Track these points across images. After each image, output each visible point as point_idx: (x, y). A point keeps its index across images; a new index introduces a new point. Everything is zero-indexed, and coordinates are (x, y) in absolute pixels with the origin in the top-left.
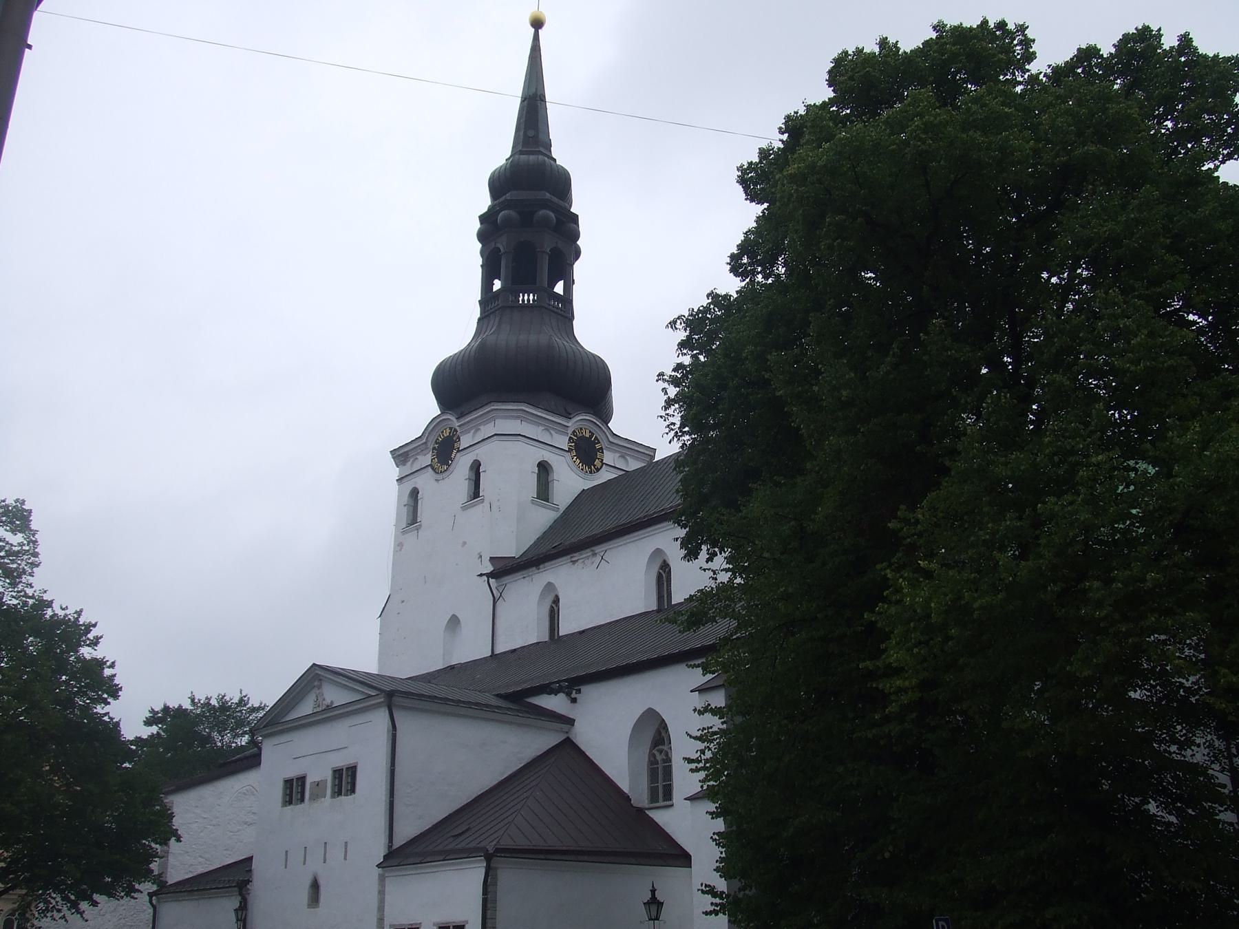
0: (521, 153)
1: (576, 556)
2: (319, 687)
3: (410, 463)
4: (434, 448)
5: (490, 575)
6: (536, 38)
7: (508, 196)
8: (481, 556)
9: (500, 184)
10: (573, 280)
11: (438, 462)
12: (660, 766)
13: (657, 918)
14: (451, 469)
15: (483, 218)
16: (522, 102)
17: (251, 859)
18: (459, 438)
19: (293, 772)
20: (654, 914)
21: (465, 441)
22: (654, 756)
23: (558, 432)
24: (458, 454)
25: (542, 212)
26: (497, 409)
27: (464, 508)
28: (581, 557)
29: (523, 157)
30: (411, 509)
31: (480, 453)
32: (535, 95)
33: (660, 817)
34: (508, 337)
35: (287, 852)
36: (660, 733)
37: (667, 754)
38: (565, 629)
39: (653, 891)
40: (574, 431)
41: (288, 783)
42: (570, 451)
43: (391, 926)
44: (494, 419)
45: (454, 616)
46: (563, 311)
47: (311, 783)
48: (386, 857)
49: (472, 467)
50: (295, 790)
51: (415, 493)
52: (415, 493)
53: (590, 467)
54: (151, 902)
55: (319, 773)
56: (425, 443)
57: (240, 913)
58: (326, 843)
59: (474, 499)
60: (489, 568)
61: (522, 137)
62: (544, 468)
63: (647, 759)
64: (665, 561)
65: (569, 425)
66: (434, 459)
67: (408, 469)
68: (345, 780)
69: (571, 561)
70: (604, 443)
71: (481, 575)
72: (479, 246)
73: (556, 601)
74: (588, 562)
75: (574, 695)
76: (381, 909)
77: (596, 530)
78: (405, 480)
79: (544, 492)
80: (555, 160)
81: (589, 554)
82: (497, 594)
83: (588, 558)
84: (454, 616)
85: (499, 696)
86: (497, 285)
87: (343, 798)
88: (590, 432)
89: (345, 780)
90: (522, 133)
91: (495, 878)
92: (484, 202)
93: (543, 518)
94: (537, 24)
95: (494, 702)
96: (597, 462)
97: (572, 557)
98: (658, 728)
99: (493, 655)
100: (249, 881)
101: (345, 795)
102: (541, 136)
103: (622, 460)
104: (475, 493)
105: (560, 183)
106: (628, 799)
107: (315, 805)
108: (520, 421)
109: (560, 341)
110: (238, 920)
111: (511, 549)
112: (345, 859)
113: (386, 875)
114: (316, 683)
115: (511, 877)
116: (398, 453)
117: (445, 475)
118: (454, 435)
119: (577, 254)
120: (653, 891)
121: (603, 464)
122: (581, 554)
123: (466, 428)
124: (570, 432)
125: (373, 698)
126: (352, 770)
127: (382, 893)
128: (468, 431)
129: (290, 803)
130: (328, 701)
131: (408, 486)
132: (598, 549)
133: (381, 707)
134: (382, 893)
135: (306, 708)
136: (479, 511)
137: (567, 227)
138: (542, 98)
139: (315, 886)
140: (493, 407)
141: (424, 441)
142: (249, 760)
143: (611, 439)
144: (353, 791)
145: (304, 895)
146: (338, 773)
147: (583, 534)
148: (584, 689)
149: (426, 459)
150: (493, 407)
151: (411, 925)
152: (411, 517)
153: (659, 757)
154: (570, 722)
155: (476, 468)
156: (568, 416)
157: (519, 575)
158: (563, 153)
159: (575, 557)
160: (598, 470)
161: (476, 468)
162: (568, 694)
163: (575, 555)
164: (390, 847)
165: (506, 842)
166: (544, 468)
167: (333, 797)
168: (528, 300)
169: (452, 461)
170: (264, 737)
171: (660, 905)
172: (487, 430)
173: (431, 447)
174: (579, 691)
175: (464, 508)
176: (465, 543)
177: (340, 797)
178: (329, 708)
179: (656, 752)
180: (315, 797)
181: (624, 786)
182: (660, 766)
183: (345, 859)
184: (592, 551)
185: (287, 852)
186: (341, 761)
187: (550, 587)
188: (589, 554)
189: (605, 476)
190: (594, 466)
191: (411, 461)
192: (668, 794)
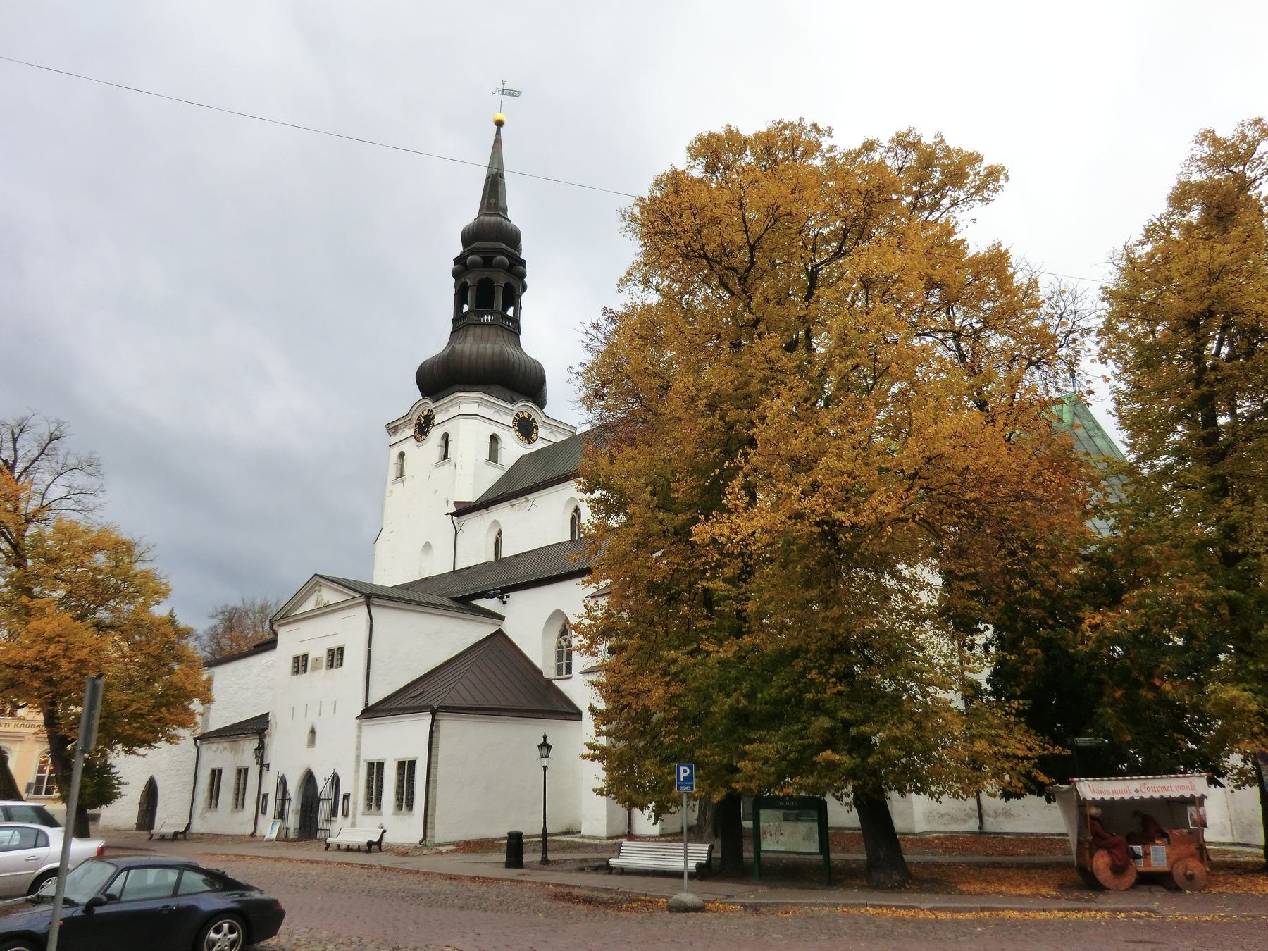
0: (485, 214)
1: (514, 502)
2: (319, 591)
4: (416, 424)
5: (453, 514)
6: (498, 132)
7: (475, 245)
9: (469, 237)
10: (521, 307)
12: (565, 650)
13: (547, 757)
15: (456, 261)
16: (487, 178)
17: (268, 714)
18: (434, 416)
19: (299, 652)
20: (544, 755)
21: (438, 419)
23: (505, 413)
25: (499, 257)
27: (437, 466)
29: (487, 218)
30: (400, 467)
31: (447, 428)
32: (496, 174)
33: (562, 685)
34: (471, 346)
36: (565, 627)
37: (569, 642)
38: (506, 552)
39: (545, 738)
41: (296, 659)
43: (365, 761)
44: (459, 403)
45: (428, 542)
46: (512, 327)
48: (363, 712)
49: (443, 438)
50: (300, 664)
51: (402, 455)
52: (402, 455)
54: (195, 744)
55: (318, 652)
57: (258, 752)
60: (453, 510)
61: (485, 205)
62: (494, 439)
63: (555, 645)
64: (577, 507)
67: (394, 439)
68: (336, 657)
70: (539, 423)
71: (447, 514)
72: (453, 280)
73: (500, 533)
74: (523, 506)
75: (505, 599)
76: (358, 748)
77: (529, 483)
79: (493, 457)
80: (509, 221)
82: (458, 528)
83: (522, 503)
84: (428, 542)
85: (452, 599)
86: (466, 308)
87: (334, 670)
89: (336, 657)
90: (486, 201)
91: (438, 727)
92: (458, 249)
93: (493, 475)
94: (499, 124)
95: (447, 602)
99: (454, 571)
100: (266, 729)
101: (336, 667)
102: (500, 203)
103: (551, 434)
105: (513, 239)
106: (540, 673)
107: (316, 674)
109: (509, 350)
110: (256, 757)
111: (471, 496)
112: (334, 712)
114: (317, 588)
115: (451, 726)
116: (391, 426)
119: (524, 288)
120: (545, 738)
123: (438, 409)
124: (514, 414)
126: (341, 650)
127: (359, 737)
128: (440, 412)
129: (297, 673)
130: (325, 601)
131: (395, 452)
132: (530, 497)
134: (359, 737)
135: (309, 605)
136: (446, 468)
137: (516, 269)
138: (502, 176)
139: (313, 732)
142: (269, 645)
143: (544, 420)
144: (341, 664)
146: (331, 652)
147: (520, 486)
148: (512, 594)
149: (410, 431)
153: (564, 644)
154: (502, 618)
155: (446, 437)
156: (513, 402)
157: (473, 515)
158: (517, 214)
160: (534, 441)
161: (446, 437)
162: (501, 598)
164: (366, 705)
165: (448, 702)
166: (494, 439)
167: (327, 669)
168: (487, 320)
170: (280, 625)
171: (549, 747)
172: (454, 411)
174: (508, 597)
175: (437, 466)
176: (436, 492)
177: (333, 669)
178: (326, 606)
179: (563, 641)
180: (314, 669)
181: (538, 663)
182: (565, 650)
183: (334, 712)
186: (334, 644)
187: (496, 522)
189: (539, 445)
192: (569, 670)
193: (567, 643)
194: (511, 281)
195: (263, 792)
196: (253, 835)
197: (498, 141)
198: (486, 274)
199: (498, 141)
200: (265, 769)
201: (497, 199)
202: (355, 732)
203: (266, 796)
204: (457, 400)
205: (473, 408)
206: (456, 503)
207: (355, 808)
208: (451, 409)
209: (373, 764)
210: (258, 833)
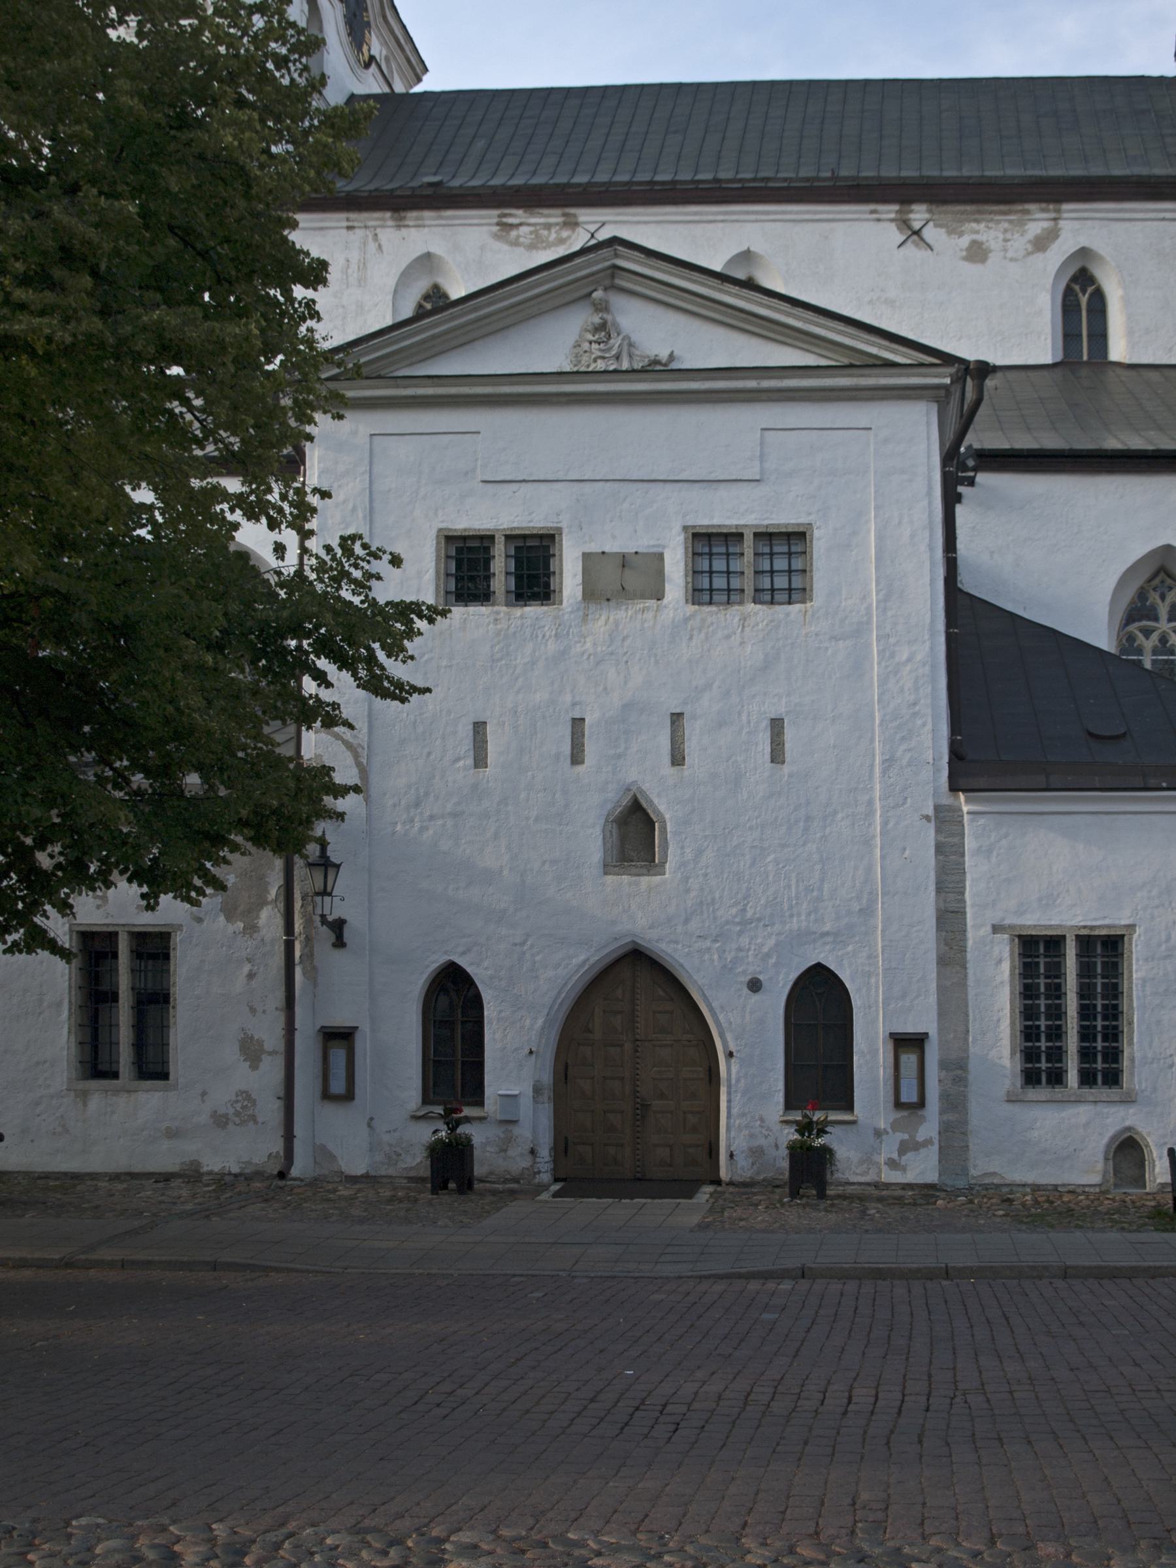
1: (518, 215)
22: (1131, 638)
28: (533, 220)
47: (586, 556)
69: (498, 224)
81: (552, 220)
83: (548, 227)
97: (505, 215)
98: (1142, 588)
122: (532, 215)
151: (1092, 928)
159: (511, 215)
163: (520, 212)
184: (564, 215)
188: (552, 220)
193: (1155, 637)
209: (1054, 943)
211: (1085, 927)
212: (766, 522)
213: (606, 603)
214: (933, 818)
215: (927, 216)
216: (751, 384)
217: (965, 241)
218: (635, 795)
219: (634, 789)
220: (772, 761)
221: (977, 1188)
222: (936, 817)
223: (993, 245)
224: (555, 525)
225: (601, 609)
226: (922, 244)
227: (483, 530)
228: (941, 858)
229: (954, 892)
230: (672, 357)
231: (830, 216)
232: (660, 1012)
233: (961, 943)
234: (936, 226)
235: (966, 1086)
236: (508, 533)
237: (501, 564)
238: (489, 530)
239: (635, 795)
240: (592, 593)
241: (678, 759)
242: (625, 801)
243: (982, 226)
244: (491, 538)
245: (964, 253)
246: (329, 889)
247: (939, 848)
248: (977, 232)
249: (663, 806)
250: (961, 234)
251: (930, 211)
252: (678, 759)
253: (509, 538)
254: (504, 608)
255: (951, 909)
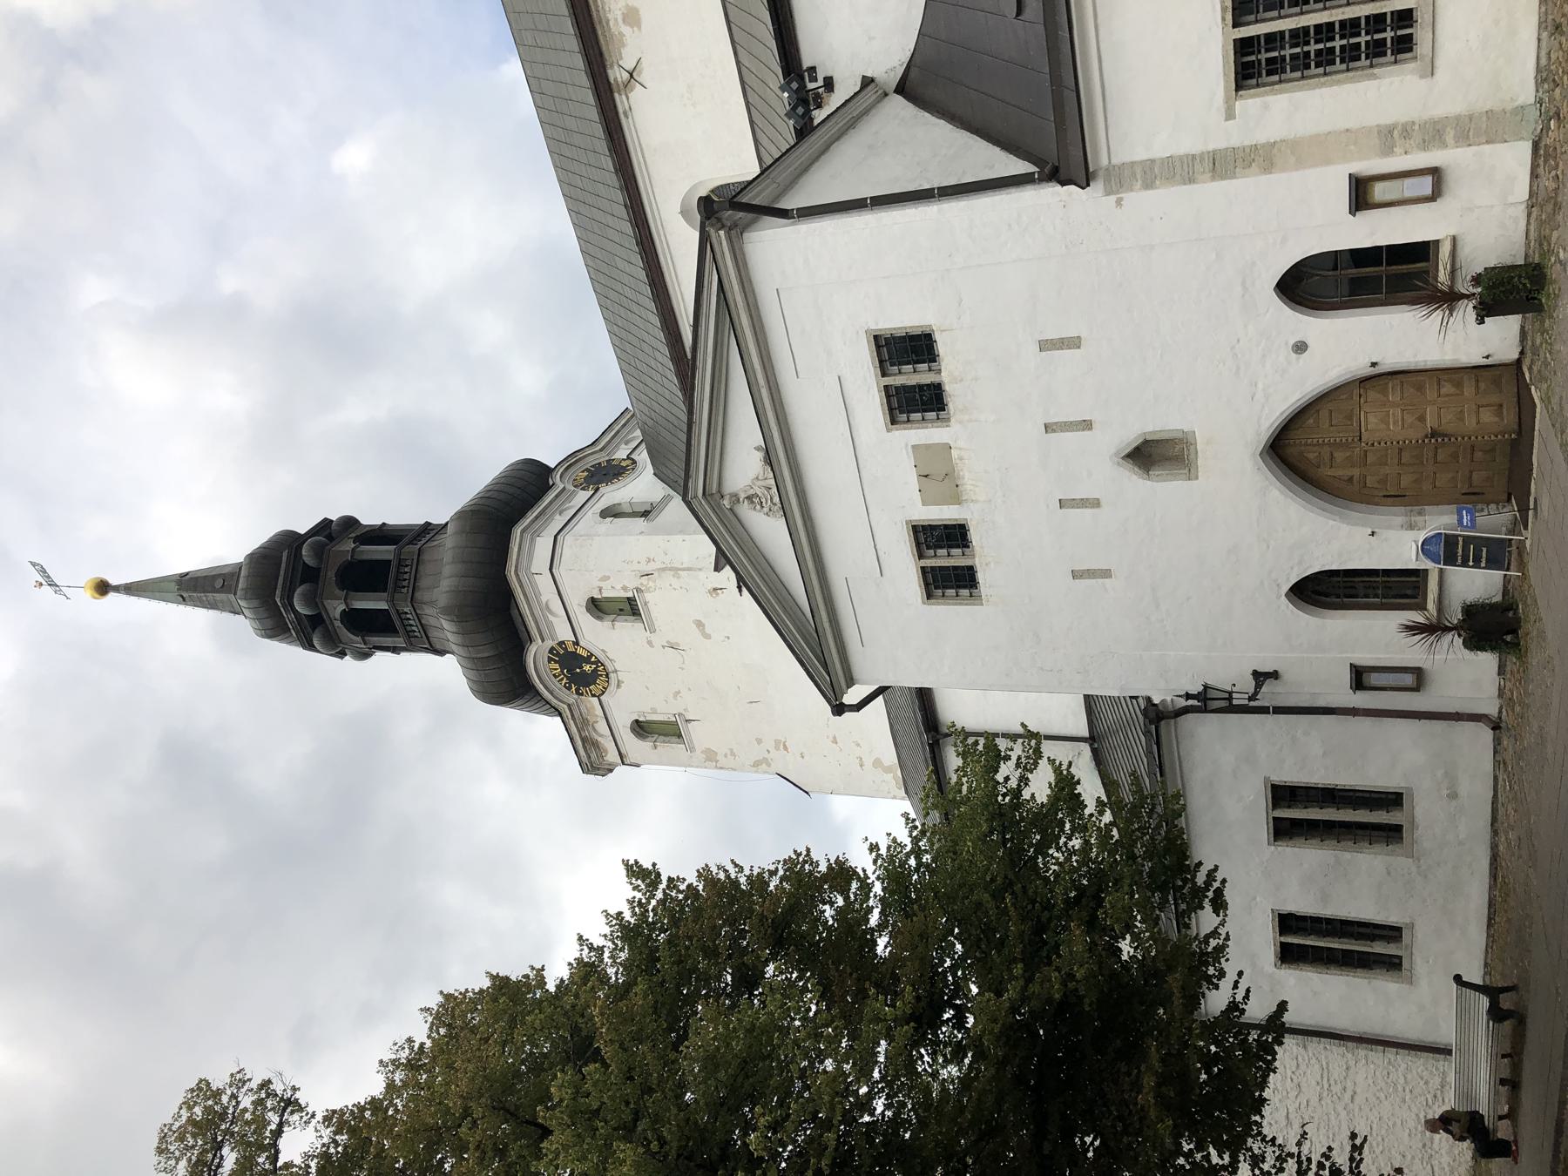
2: (735, 498)
3: (599, 739)
6: (117, 589)
8: (715, 589)
9: (276, 625)
11: (595, 683)
14: (602, 658)
16: (184, 600)
18: (561, 643)
21: (565, 634)
24: (581, 643)
26: (516, 567)
35: (1076, 575)
40: (575, 486)
42: (597, 490)
48: (1063, 183)
51: (641, 728)
52: (641, 728)
53: (628, 470)
56: (569, 705)
58: (1048, 428)
59: (640, 615)
62: (611, 513)
65: (562, 486)
66: (591, 691)
70: (602, 458)
78: (623, 751)
88: (583, 472)
90: (218, 596)
94: (103, 588)
96: (624, 464)
104: (630, 608)
107: (970, 477)
108: (538, 538)
113: (1104, 161)
114: (726, 502)
117: (610, 668)
118: (558, 654)
121: (628, 457)
125: (725, 281)
128: (550, 625)
131: (630, 742)
133: (742, 249)
136: (655, 602)
140: (512, 573)
141: (565, 706)
145: (1163, 490)
148: (806, 64)
150: (512, 573)
152: (675, 739)
155: (597, 607)
160: (634, 462)
161: (597, 607)
169: (592, 655)
173: (576, 696)
185: (1076, 575)
190: (628, 466)
191: (596, 737)
194: (353, 535)
195: (1348, 697)
196: (1496, 727)
197: (131, 589)
198: (331, 574)
199: (131, 589)
200: (1270, 694)
201: (214, 577)
202: (1139, 200)
203: (1360, 677)
204: (525, 580)
205: (543, 545)
206: (717, 568)
207: (1406, 130)
208: (544, 599)
209: (1243, 47)
210: (1492, 709)
211: (1224, 19)
212: (872, 369)
213: (960, 487)
214: (1118, 196)
215: (616, 67)
216: (765, 392)
217: (626, 30)
218: (1123, 458)
219: (1116, 459)
220: (1079, 347)
221: (1540, 94)
222: (1118, 192)
223: (621, 4)
224: (905, 527)
225: (966, 490)
226: (638, 69)
227: (918, 574)
228: (1158, 182)
229: (1193, 166)
230: (757, 449)
231: (638, 149)
232: (1331, 420)
233: (1248, 150)
234: (621, 59)
235: (1413, 123)
236: (917, 557)
237: (944, 559)
238: (917, 571)
239: (1123, 458)
240: (956, 498)
241: (1087, 425)
242: (1129, 465)
243: (610, 16)
244: (923, 569)
245: (635, 29)
246: (1227, 695)
247: (1149, 185)
248: (616, 20)
249: (1130, 435)
250: (621, 34)
251: (612, 66)
252: (1087, 425)
253: (921, 556)
254: (977, 559)
255: (1211, 165)
